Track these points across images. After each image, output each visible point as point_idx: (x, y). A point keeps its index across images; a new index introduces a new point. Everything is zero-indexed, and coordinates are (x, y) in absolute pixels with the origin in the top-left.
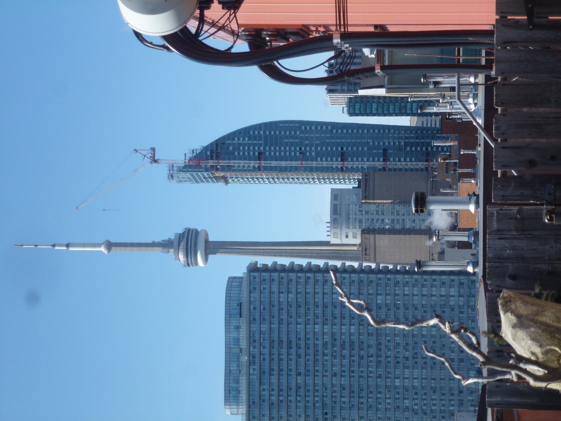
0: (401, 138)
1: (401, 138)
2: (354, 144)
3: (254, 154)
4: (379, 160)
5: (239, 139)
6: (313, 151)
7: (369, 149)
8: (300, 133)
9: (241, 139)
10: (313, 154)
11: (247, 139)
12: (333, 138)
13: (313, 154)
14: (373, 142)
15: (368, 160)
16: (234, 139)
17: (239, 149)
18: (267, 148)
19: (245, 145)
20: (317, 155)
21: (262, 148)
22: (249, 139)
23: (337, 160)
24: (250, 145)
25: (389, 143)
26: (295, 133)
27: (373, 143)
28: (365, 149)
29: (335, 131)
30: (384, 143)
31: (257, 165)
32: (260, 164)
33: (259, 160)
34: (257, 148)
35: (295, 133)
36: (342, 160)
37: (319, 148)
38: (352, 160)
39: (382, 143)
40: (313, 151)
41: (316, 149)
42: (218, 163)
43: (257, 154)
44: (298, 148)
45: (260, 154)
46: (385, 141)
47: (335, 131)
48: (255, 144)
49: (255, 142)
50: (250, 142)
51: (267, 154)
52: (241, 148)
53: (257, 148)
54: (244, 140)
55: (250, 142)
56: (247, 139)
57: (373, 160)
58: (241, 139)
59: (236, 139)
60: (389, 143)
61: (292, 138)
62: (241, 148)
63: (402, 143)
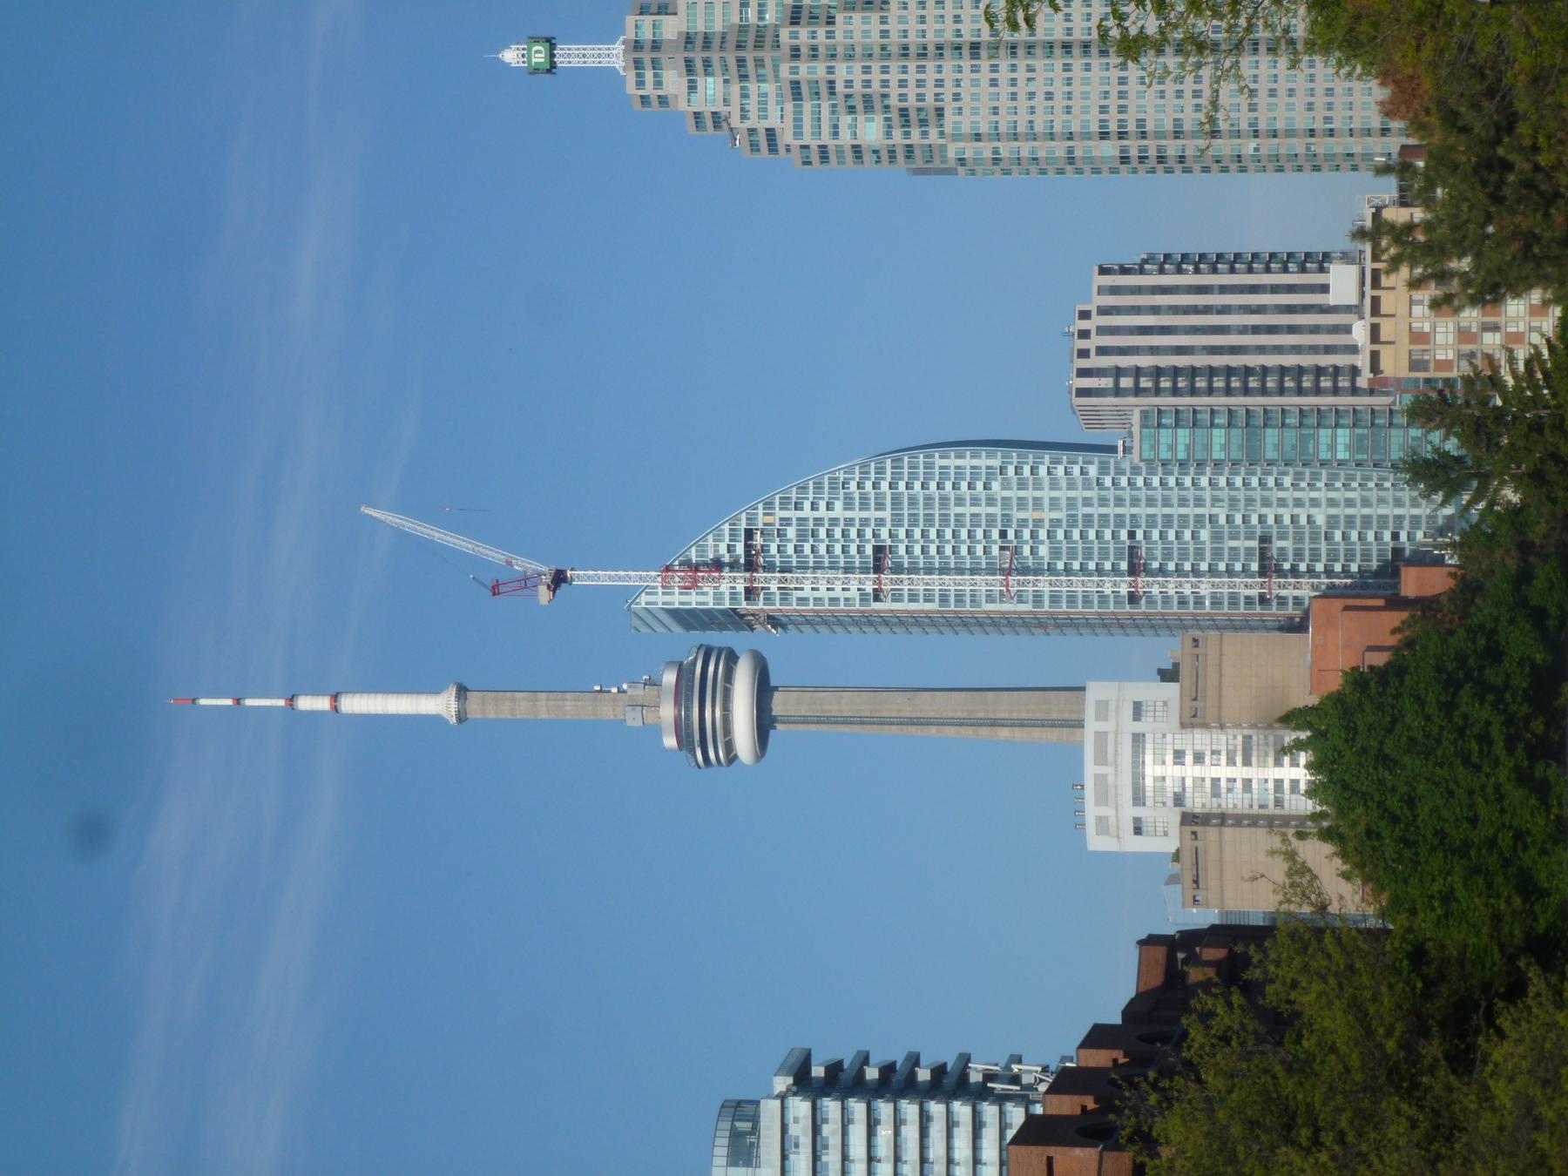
3: (860, 550)
5: (814, 507)
6: (1042, 542)
7: (1217, 537)
9: (822, 505)
10: (1043, 551)
11: (838, 505)
12: (1103, 502)
13: (1043, 551)
16: (798, 506)
17: (814, 534)
18: (902, 533)
21: (884, 533)
22: (848, 505)
23: (1115, 570)
24: (849, 522)
26: (986, 487)
27: (1229, 519)
28: (1205, 535)
29: (1108, 481)
30: (1262, 519)
31: (869, 588)
32: (879, 581)
33: (878, 569)
34: (868, 533)
35: (986, 487)
36: (1133, 570)
37: (1060, 534)
39: (1254, 520)
40: (1042, 542)
41: (1050, 535)
42: (753, 580)
43: (869, 550)
44: (995, 534)
45: (878, 550)
46: (1264, 511)
47: (1108, 481)
48: (865, 522)
49: (864, 514)
50: (849, 514)
51: (902, 550)
52: (822, 533)
53: (868, 533)
54: (829, 507)
55: (849, 514)
56: (838, 505)
58: (822, 505)
59: (807, 505)
61: (975, 501)
62: (822, 533)
63: (1320, 520)
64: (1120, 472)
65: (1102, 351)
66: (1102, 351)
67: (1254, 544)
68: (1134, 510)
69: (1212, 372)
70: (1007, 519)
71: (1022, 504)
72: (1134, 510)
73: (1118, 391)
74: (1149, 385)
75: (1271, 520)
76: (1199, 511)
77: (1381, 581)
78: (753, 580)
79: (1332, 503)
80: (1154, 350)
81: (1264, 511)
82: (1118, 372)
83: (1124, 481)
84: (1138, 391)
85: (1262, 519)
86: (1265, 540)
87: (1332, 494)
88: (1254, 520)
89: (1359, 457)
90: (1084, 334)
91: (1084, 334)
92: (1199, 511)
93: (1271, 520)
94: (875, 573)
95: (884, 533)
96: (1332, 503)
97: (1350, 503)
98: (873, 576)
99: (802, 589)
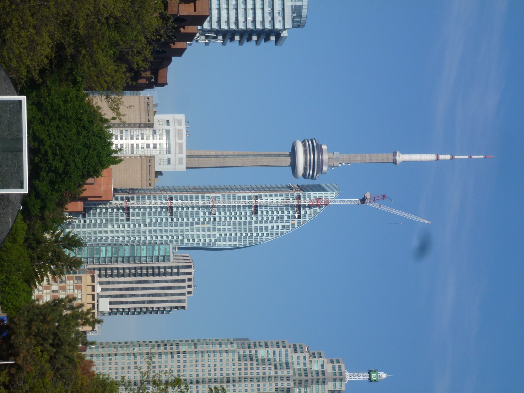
3: (262, 213)
6: (202, 217)
7: (144, 220)
10: (201, 214)
11: (270, 228)
12: (182, 231)
13: (201, 214)
18: (249, 219)
21: (254, 219)
22: (267, 227)
23: (177, 208)
24: (266, 222)
26: (221, 235)
27: (140, 226)
28: (148, 220)
30: (129, 226)
31: (259, 200)
33: (256, 206)
34: (260, 218)
35: (221, 235)
37: (196, 219)
39: (132, 226)
40: (202, 217)
41: (199, 219)
42: (298, 202)
43: (259, 213)
44: (217, 219)
45: (256, 213)
46: (129, 229)
48: (261, 222)
49: (261, 225)
50: (266, 225)
51: (248, 213)
52: (275, 218)
53: (260, 218)
55: (266, 225)
56: (270, 228)
61: (224, 230)
62: (275, 218)
63: (110, 226)
64: (176, 241)
65: (183, 281)
66: (183, 281)
67: (131, 218)
68: (171, 228)
69: (147, 275)
70: (214, 224)
71: (209, 229)
72: (171, 228)
73: (178, 267)
75: (126, 226)
76: (150, 228)
77: (89, 206)
78: (298, 202)
79: (106, 232)
80: (166, 281)
81: (129, 229)
82: (178, 274)
83: (175, 238)
84: (171, 268)
85: (129, 226)
86: (128, 219)
88: (132, 226)
89: (97, 247)
90: (189, 286)
91: (189, 286)
92: (150, 228)
93: (126, 226)
94: (257, 205)
95: (254, 219)
96: (106, 232)
97: (100, 232)
98: (258, 204)
99: (281, 199)
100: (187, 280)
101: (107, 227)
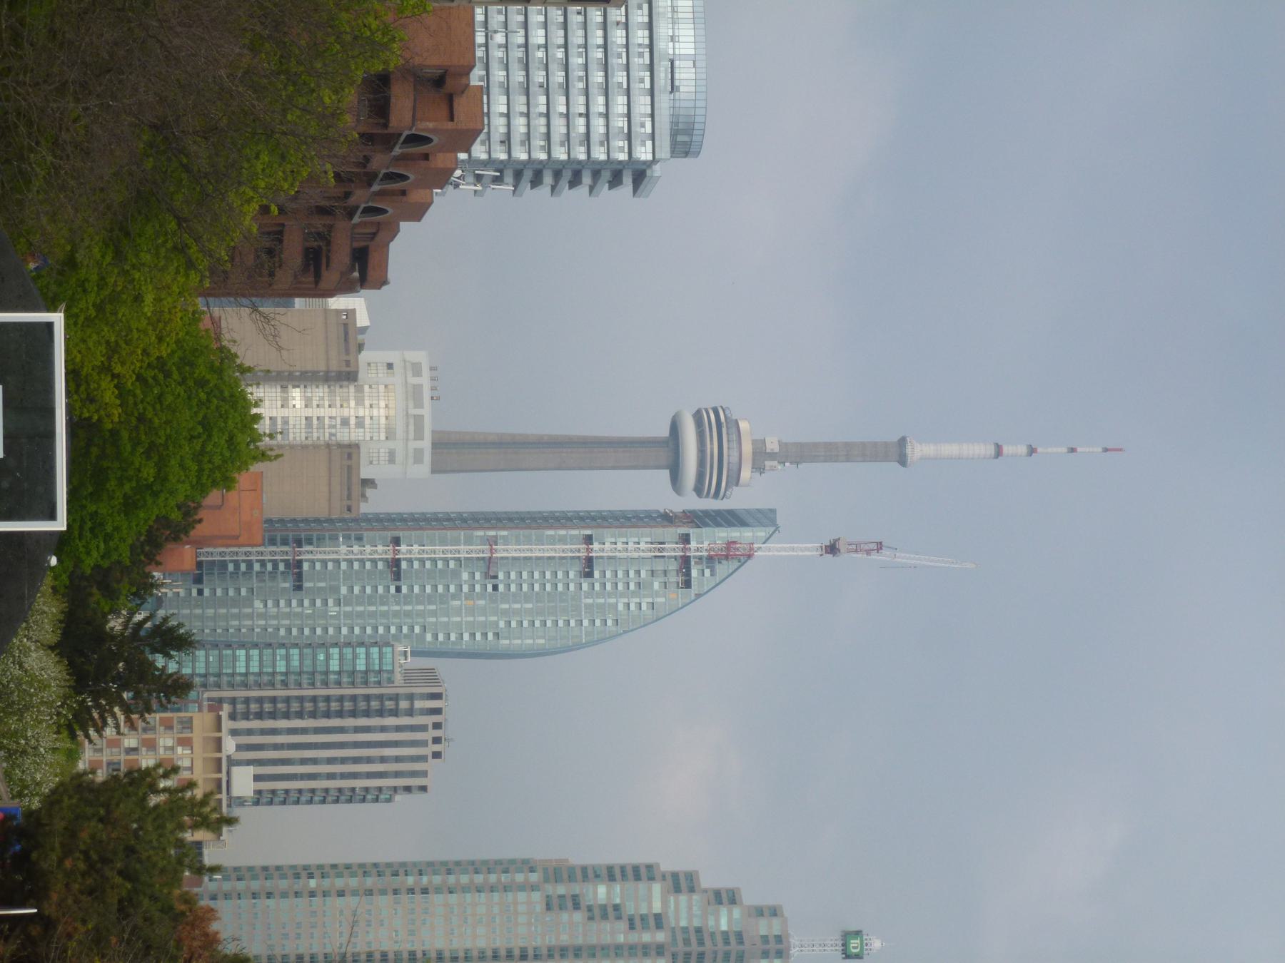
0: (264, 616)
1: (264, 616)
2: (371, 600)
4: (313, 562)
7: (336, 590)
8: (497, 623)
9: (632, 607)
10: (465, 576)
11: (621, 607)
12: (421, 614)
13: (465, 576)
14: (327, 605)
15: (337, 562)
17: (639, 585)
19: (622, 595)
20: (456, 574)
21: (585, 586)
23: (410, 561)
25: (289, 604)
28: (344, 590)
29: (417, 629)
30: (301, 604)
31: (596, 546)
34: (597, 586)
36: (397, 563)
38: (374, 562)
39: (306, 603)
42: (683, 550)
43: (597, 574)
44: (501, 588)
45: (589, 575)
47: (417, 629)
48: (598, 595)
50: (613, 601)
51: (572, 575)
52: (632, 586)
53: (597, 586)
55: (613, 601)
56: (621, 607)
57: (324, 562)
60: (289, 604)
62: (632, 586)
63: (258, 604)
65: (423, 728)
66: (423, 728)
67: (307, 585)
69: (340, 714)
73: (411, 697)
74: (387, 703)
77: (210, 559)
78: (683, 550)
79: (251, 617)
80: (383, 729)
82: (410, 712)
83: (405, 630)
84: (396, 698)
85: (301, 604)
86: (299, 588)
87: (249, 623)
89: (229, 652)
91: (437, 740)
93: (294, 603)
94: (592, 557)
96: (251, 617)
97: (238, 617)
98: (593, 554)
99: (646, 543)
100: (430, 727)
101: (252, 606)
